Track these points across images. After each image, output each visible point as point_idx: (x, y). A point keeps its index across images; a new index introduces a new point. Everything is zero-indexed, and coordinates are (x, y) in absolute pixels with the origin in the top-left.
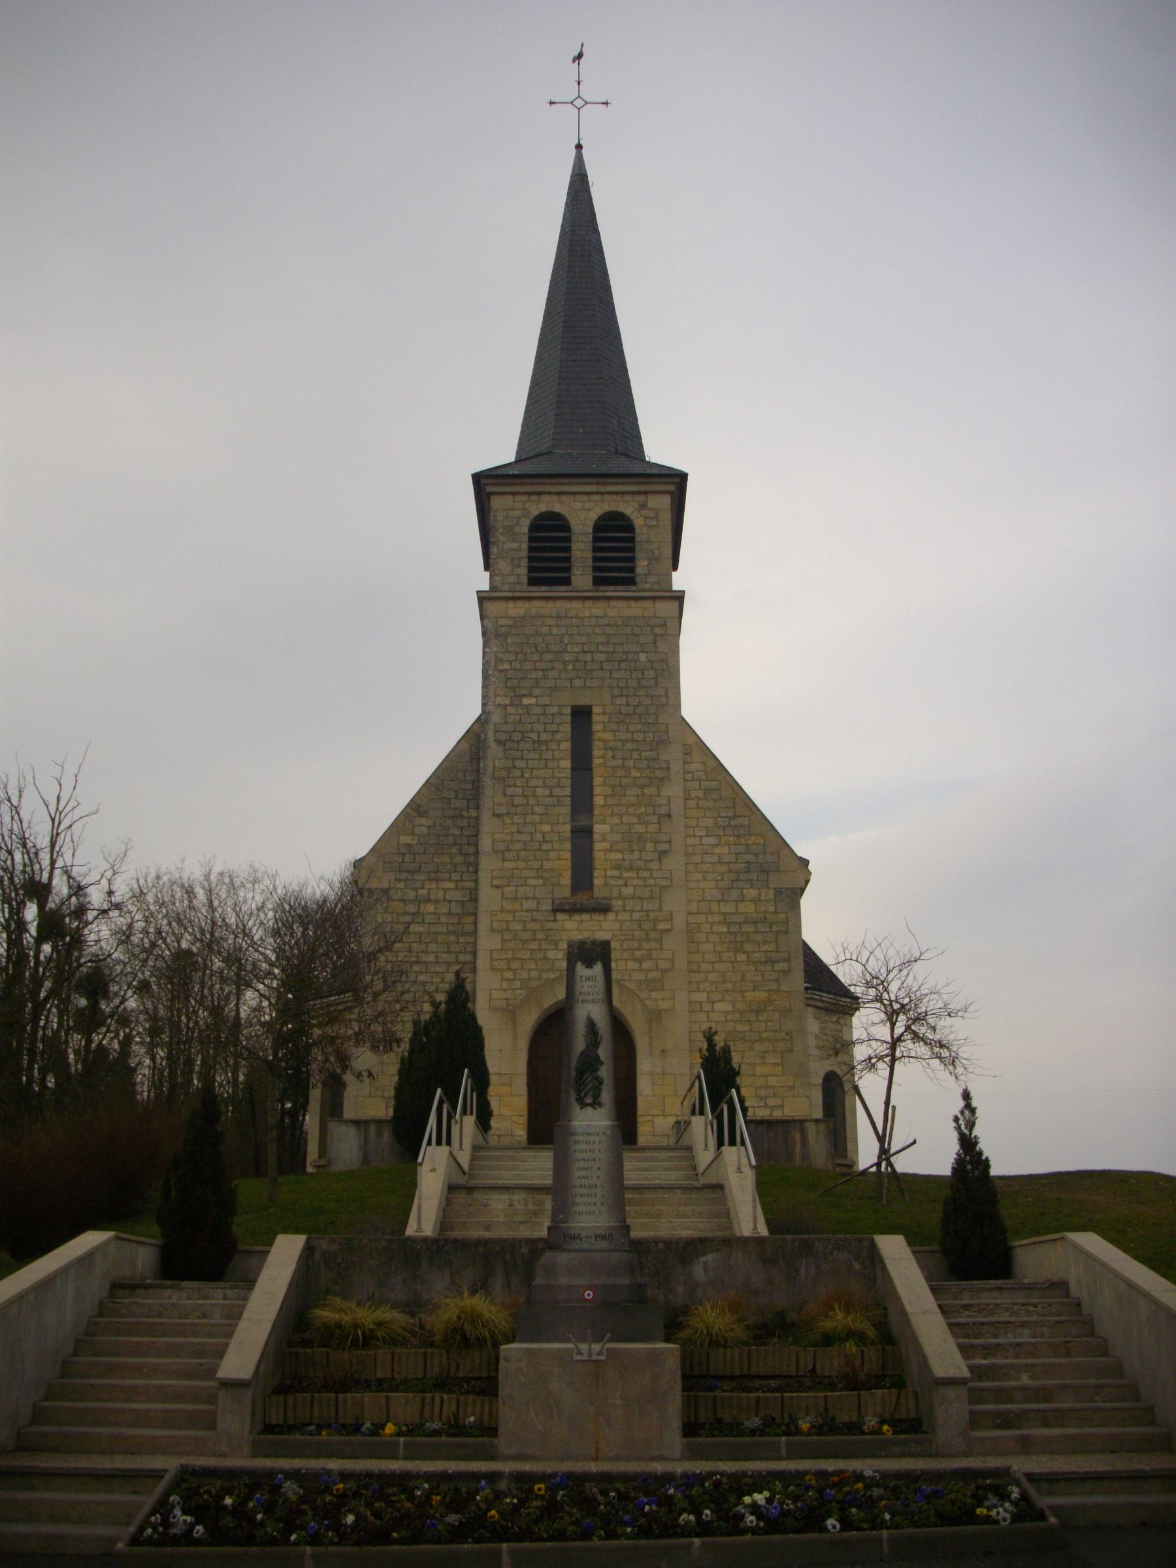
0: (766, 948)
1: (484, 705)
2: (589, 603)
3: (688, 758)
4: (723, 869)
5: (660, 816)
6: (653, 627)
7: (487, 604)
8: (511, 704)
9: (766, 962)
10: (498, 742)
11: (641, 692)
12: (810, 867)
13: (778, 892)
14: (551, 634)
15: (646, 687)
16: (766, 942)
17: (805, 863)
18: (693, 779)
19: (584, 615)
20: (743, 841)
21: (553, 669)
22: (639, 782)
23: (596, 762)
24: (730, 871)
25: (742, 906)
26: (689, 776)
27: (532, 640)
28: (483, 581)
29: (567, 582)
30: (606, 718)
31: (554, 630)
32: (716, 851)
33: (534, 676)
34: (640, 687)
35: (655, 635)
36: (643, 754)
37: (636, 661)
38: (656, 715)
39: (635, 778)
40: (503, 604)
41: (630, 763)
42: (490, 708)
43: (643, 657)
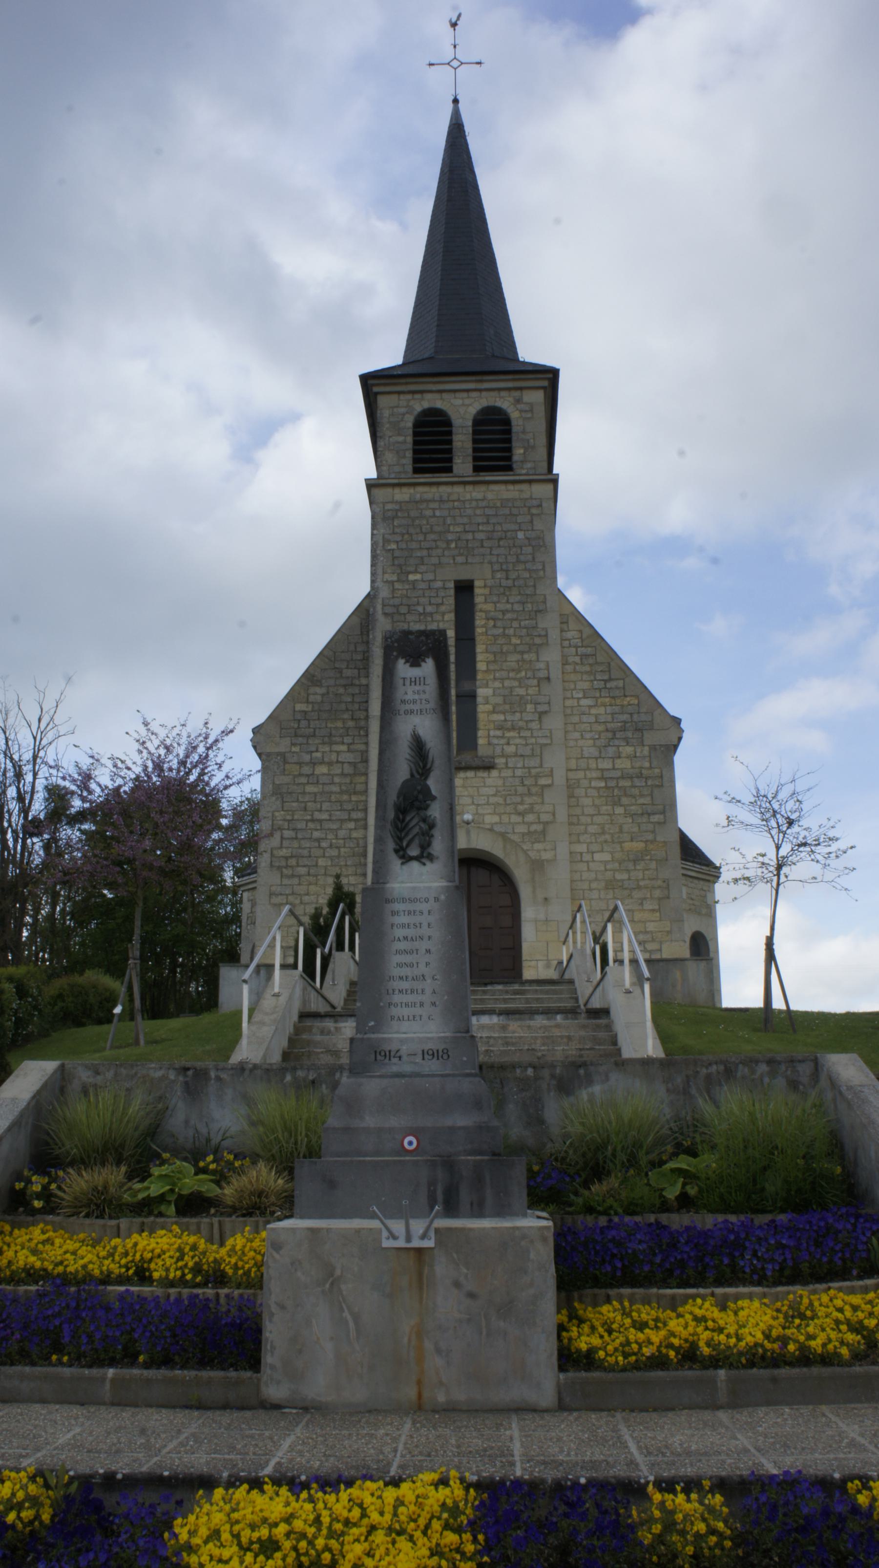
0: (641, 801)
1: (373, 582)
2: (469, 488)
3: (565, 626)
4: (601, 728)
5: (540, 680)
6: (529, 508)
7: (376, 491)
8: (398, 581)
9: (642, 814)
10: (386, 614)
11: (521, 567)
12: (683, 725)
13: (653, 748)
14: (434, 516)
15: (525, 562)
16: (642, 796)
17: (677, 721)
18: (570, 646)
19: (465, 495)
20: (618, 702)
21: (437, 547)
22: (519, 648)
23: (479, 630)
24: (607, 730)
25: (618, 761)
26: (566, 643)
27: (417, 522)
28: (373, 474)
29: (449, 470)
30: (487, 591)
31: (438, 513)
32: (593, 711)
33: (419, 554)
34: (518, 561)
35: (532, 515)
36: (523, 623)
37: (515, 538)
38: (534, 586)
39: (516, 645)
40: (389, 490)
41: (511, 632)
42: (379, 584)
43: (520, 535)
